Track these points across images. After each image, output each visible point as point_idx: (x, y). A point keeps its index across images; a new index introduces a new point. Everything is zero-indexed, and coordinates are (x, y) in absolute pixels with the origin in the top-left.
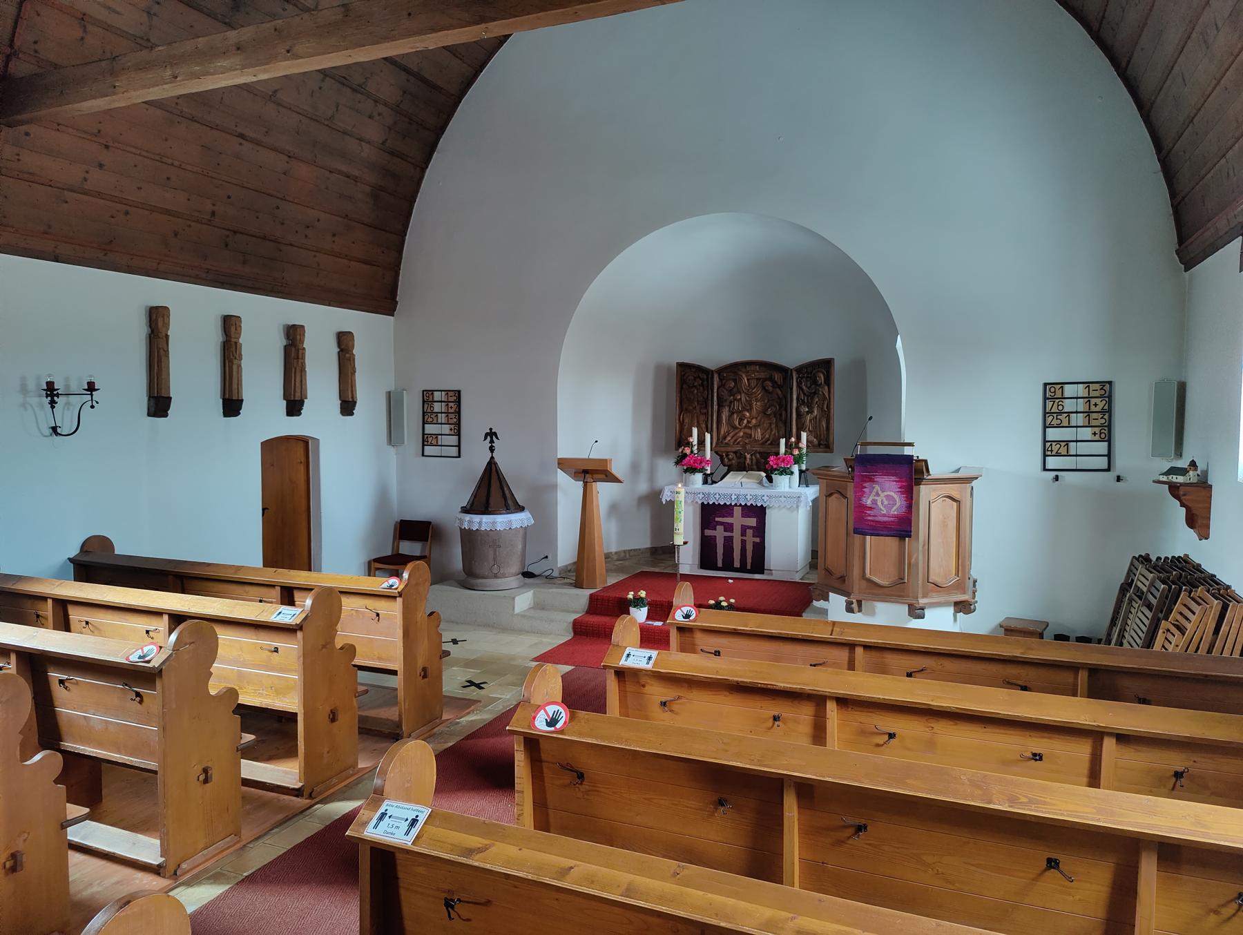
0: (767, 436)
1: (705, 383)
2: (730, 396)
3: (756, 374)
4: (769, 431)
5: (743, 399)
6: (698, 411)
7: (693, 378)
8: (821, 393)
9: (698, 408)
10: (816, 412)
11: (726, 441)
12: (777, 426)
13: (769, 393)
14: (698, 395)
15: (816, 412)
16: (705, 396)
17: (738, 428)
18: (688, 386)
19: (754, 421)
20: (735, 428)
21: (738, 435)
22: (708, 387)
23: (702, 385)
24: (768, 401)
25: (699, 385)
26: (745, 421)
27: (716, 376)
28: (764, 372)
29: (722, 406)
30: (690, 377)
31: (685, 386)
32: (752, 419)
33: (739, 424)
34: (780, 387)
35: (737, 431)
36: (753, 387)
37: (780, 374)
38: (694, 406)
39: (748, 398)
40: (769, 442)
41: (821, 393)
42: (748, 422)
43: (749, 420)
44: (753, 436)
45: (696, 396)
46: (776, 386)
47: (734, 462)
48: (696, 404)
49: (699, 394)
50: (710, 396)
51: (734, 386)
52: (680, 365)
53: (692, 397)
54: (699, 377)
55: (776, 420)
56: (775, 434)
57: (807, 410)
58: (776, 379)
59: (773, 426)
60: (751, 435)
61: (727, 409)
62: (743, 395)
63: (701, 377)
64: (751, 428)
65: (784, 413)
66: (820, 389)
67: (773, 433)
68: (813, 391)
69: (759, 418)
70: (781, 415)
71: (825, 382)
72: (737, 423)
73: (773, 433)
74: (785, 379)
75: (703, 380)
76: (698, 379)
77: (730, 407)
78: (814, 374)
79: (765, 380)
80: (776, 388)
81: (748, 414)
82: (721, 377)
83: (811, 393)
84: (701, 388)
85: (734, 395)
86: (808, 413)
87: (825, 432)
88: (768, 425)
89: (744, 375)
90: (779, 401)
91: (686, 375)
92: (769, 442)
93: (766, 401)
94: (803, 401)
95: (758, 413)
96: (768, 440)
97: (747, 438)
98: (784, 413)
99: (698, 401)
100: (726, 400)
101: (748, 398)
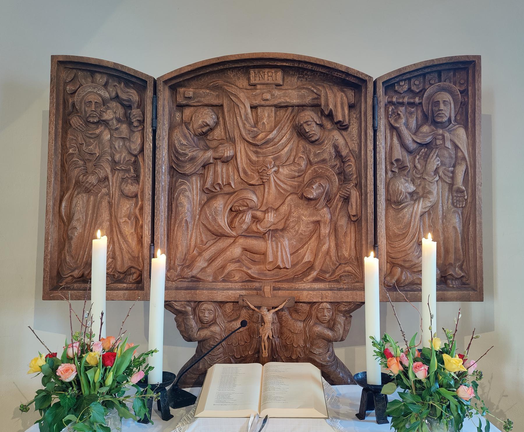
0: (308, 258)
1: (135, 112)
2: (207, 148)
3: (277, 93)
4: (313, 243)
5: (242, 161)
6: (115, 190)
7: (100, 100)
8: (448, 144)
9: (114, 180)
10: (435, 192)
11: (194, 272)
12: (335, 230)
13: (313, 142)
14: (112, 147)
15: (435, 192)
16: (135, 147)
17: (229, 236)
18: (87, 123)
19: (271, 217)
20: (220, 235)
21: (228, 254)
22: (142, 122)
23: (127, 119)
24: (310, 163)
25: (119, 120)
26: (248, 218)
27: (165, 95)
28: (299, 88)
29: (184, 175)
30: (92, 98)
31: (75, 121)
32: (266, 212)
33: (231, 224)
34: (342, 127)
35: (222, 244)
36: (268, 127)
37: (340, 94)
38: (102, 175)
39: (254, 158)
40: (314, 274)
41: (448, 144)
42: (255, 219)
43: (259, 214)
44: (270, 258)
45: (107, 149)
46: (328, 125)
47: (215, 329)
48: (108, 170)
49: (119, 144)
50: (149, 145)
51: (217, 124)
52: (60, 63)
53: (97, 152)
54: (117, 98)
55: (332, 214)
56: (328, 252)
57: (412, 188)
58: (331, 107)
59: (325, 230)
60: (264, 254)
61: (196, 183)
62: (241, 147)
63: (124, 96)
64: (262, 236)
65: (354, 194)
66: (447, 135)
67: (325, 248)
68: (428, 139)
69: (284, 209)
70: (347, 200)
71: (456, 120)
72: (223, 221)
73: (325, 248)
74: (351, 107)
75: (127, 106)
76: (114, 104)
77: (203, 177)
78: (430, 97)
79: (302, 107)
80: (330, 130)
81: (255, 198)
82: (181, 100)
83: (421, 145)
84: (124, 127)
85: (215, 149)
86: (414, 196)
87: (460, 245)
88: (311, 227)
89: (242, 95)
90: (338, 163)
91: (81, 93)
92: (314, 274)
93: (303, 164)
94: (403, 168)
95: (282, 196)
96: (311, 267)
97: (254, 262)
98: (354, 194)
99: (114, 163)
100: (192, 159)
101: (254, 158)
